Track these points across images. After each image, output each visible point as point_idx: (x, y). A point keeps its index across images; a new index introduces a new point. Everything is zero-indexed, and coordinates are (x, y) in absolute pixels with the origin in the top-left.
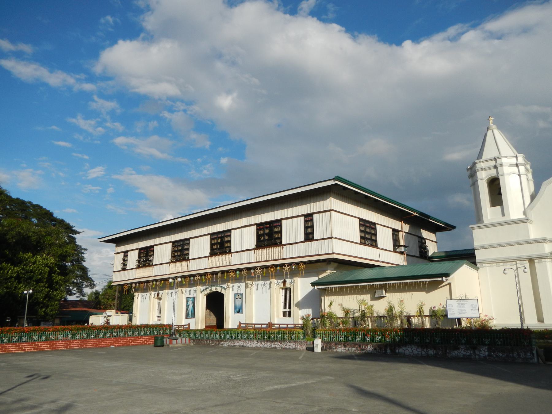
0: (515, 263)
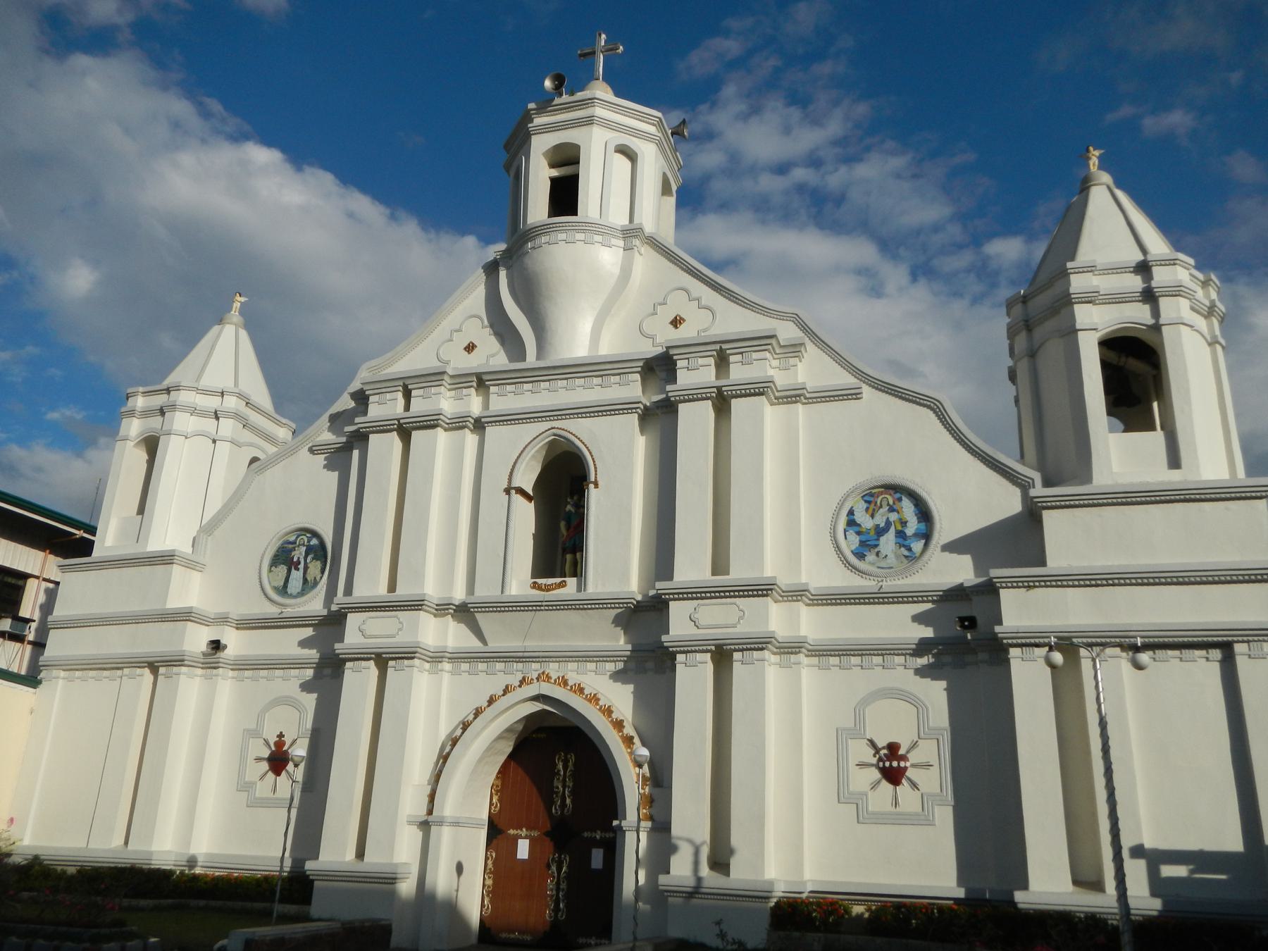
0: (119, 672)
